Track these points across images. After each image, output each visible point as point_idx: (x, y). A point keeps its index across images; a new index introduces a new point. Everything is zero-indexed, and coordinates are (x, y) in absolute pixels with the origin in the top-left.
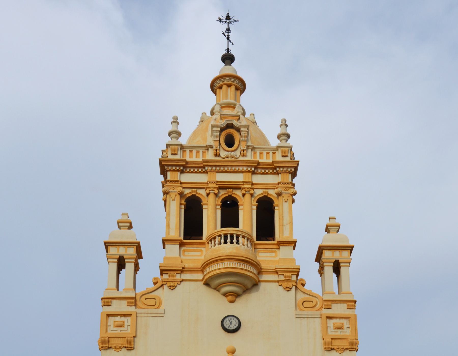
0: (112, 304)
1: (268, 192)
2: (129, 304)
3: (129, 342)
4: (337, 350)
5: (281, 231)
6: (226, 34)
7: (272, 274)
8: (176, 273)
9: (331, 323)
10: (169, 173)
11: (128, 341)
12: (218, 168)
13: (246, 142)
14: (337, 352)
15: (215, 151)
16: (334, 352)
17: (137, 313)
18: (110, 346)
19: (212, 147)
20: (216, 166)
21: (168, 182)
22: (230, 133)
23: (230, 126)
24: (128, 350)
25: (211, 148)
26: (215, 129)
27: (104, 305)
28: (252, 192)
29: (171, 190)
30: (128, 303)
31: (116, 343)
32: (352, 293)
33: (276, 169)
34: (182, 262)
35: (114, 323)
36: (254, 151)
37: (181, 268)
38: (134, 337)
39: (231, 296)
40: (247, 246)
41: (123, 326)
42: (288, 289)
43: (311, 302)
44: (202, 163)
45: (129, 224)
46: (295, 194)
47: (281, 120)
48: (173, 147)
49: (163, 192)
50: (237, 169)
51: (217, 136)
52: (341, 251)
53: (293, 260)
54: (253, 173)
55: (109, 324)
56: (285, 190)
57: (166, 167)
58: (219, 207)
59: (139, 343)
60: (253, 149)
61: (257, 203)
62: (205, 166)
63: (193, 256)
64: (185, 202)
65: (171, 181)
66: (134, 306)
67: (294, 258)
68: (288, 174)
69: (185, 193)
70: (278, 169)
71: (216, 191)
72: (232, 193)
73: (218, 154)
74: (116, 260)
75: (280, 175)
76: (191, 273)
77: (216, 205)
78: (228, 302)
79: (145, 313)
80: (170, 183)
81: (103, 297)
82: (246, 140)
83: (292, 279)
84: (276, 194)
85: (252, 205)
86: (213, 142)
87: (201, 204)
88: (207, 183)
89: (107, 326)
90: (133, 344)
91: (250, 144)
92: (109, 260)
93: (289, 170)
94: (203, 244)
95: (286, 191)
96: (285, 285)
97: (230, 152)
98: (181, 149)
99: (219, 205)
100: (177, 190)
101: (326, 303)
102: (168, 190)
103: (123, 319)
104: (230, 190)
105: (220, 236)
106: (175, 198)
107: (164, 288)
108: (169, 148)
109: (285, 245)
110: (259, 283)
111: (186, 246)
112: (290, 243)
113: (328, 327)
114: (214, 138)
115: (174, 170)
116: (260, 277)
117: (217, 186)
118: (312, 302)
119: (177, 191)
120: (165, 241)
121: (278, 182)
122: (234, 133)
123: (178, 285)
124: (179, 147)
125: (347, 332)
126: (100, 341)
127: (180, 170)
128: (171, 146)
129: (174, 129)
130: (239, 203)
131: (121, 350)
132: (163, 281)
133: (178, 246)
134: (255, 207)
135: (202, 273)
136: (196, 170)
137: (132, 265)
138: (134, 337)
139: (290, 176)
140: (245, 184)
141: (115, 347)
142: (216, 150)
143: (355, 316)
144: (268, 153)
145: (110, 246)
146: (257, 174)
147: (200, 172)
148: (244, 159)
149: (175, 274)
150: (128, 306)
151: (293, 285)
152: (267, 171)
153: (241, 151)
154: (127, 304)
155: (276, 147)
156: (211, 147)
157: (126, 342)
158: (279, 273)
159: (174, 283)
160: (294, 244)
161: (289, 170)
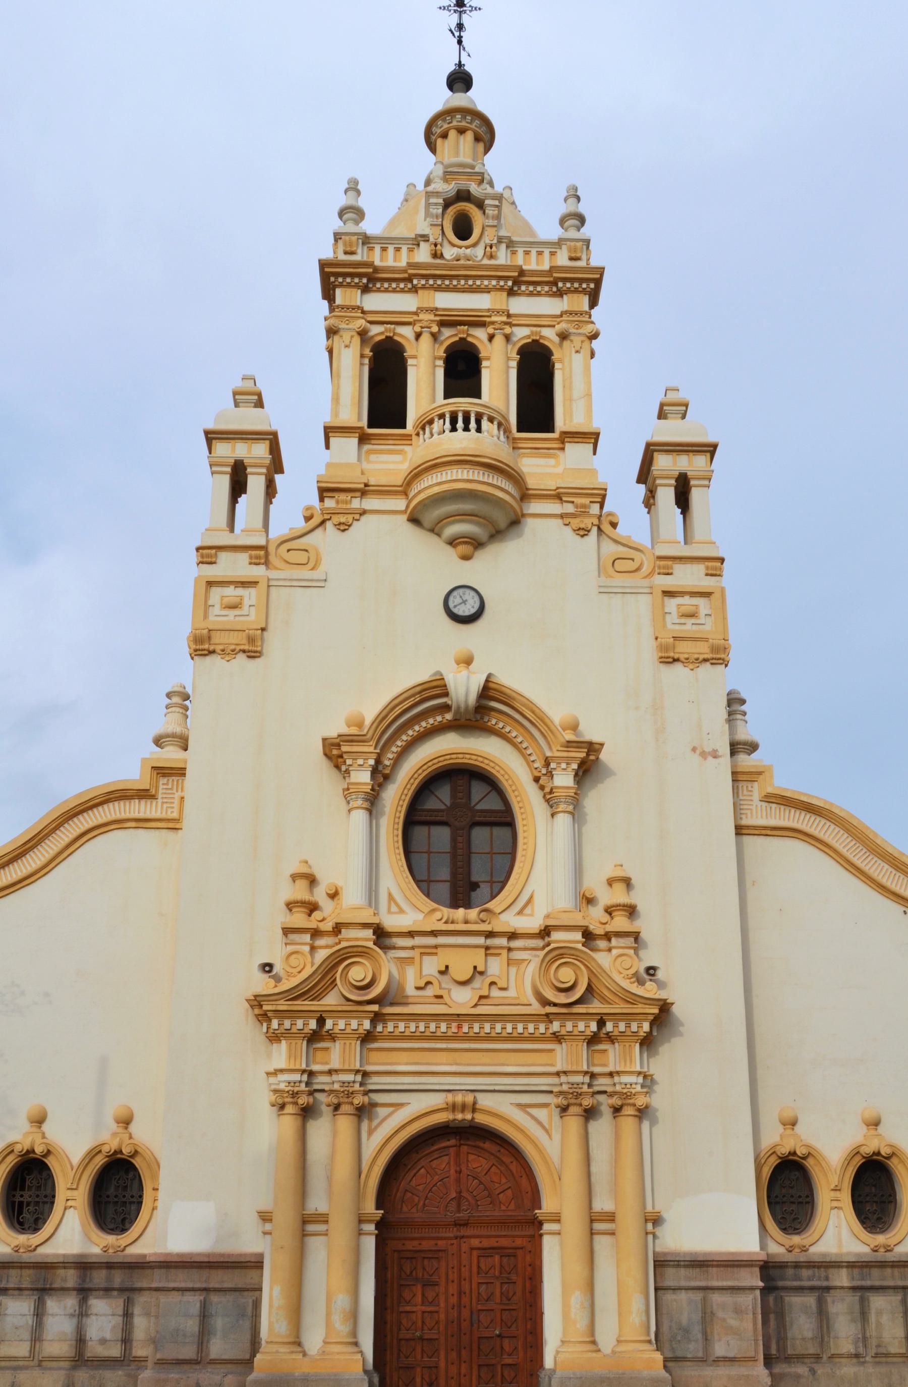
0: (218, 561)
1: (540, 332)
2: (253, 561)
4: (686, 662)
5: (568, 413)
6: (457, 34)
7: (548, 501)
8: (352, 497)
9: (672, 604)
10: (338, 291)
11: (249, 639)
12: (439, 282)
13: (495, 229)
14: (685, 666)
15: (433, 246)
16: (678, 667)
17: (269, 580)
18: (212, 648)
19: (428, 239)
20: (435, 277)
21: (336, 310)
22: (464, 210)
23: (463, 196)
24: (249, 657)
25: (424, 241)
26: (433, 200)
27: (202, 563)
28: (508, 330)
29: (343, 326)
30: (251, 557)
31: (226, 641)
32: (715, 543)
33: (556, 285)
34: (363, 473)
35: (222, 600)
36: (511, 249)
37: (362, 486)
38: (263, 630)
40: (498, 438)
41: (240, 606)
42: (582, 533)
43: (631, 561)
44: (405, 271)
45: (256, 397)
46: (594, 336)
47: (568, 187)
48: (347, 238)
49: (326, 329)
50: (478, 282)
51: (437, 217)
52: (691, 454)
53: (593, 472)
54: (511, 293)
55: (210, 602)
56: (576, 326)
57: (332, 279)
58: (441, 363)
59: (273, 643)
60: (511, 244)
61: (517, 354)
62: (413, 277)
63: (386, 462)
64: (371, 351)
65: (342, 307)
66: (263, 564)
67: (595, 467)
68: (581, 295)
69: (371, 334)
70: (560, 285)
71: (435, 329)
72: (468, 335)
73: (439, 252)
74: (229, 469)
75: (565, 296)
76: (382, 497)
77: (436, 358)
79: (285, 579)
80: (340, 311)
81: (199, 543)
82: (496, 224)
83: (591, 512)
84: (557, 335)
85: (508, 359)
86: (430, 227)
87: (404, 356)
88: (416, 313)
89: (207, 607)
90: (259, 643)
91: (503, 233)
92: (214, 469)
93: (584, 286)
94: (408, 437)
95: (577, 329)
96: (576, 523)
97: (463, 248)
98: (363, 244)
99: (440, 358)
100: (355, 325)
101: (662, 563)
102: (336, 325)
103: (240, 591)
104: (462, 327)
105: (442, 416)
106: (350, 342)
107: (325, 529)
108: (339, 240)
109: (576, 440)
110: (523, 520)
111: (373, 442)
112: (586, 436)
113: (666, 613)
114: (432, 220)
115: (349, 285)
116: (525, 506)
117: (438, 318)
118: (633, 560)
119: (355, 327)
120: (329, 430)
121: (562, 312)
122: (471, 211)
123: (355, 522)
124: (360, 239)
125: (707, 626)
126: (191, 639)
127: (361, 284)
128: (343, 237)
129: (351, 202)
130: (480, 353)
131: (235, 658)
132: (324, 512)
133: (355, 441)
134: (514, 364)
135: (404, 497)
136: (394, 285)
137: (262, 479)
138: (263, 630)
139: (585, 300)
140: (493, 314)
141: (223, 650)
142: (436, 245)
143: (723, 590)
144: (540, 253)
145: (217, 441)
146: (519, 295)
147: (402, 291)
148: (493, 262)
149: (349, 497)
150: (250, 563)
151: (592, 523)
152: (539, 289)
153: (486, 248)
155: (557, 241)
156: (425, 237)
157: (245, 641)
158: (564, 499)
159: (346, 516)
160: (595, 438)
161: (584, 286)
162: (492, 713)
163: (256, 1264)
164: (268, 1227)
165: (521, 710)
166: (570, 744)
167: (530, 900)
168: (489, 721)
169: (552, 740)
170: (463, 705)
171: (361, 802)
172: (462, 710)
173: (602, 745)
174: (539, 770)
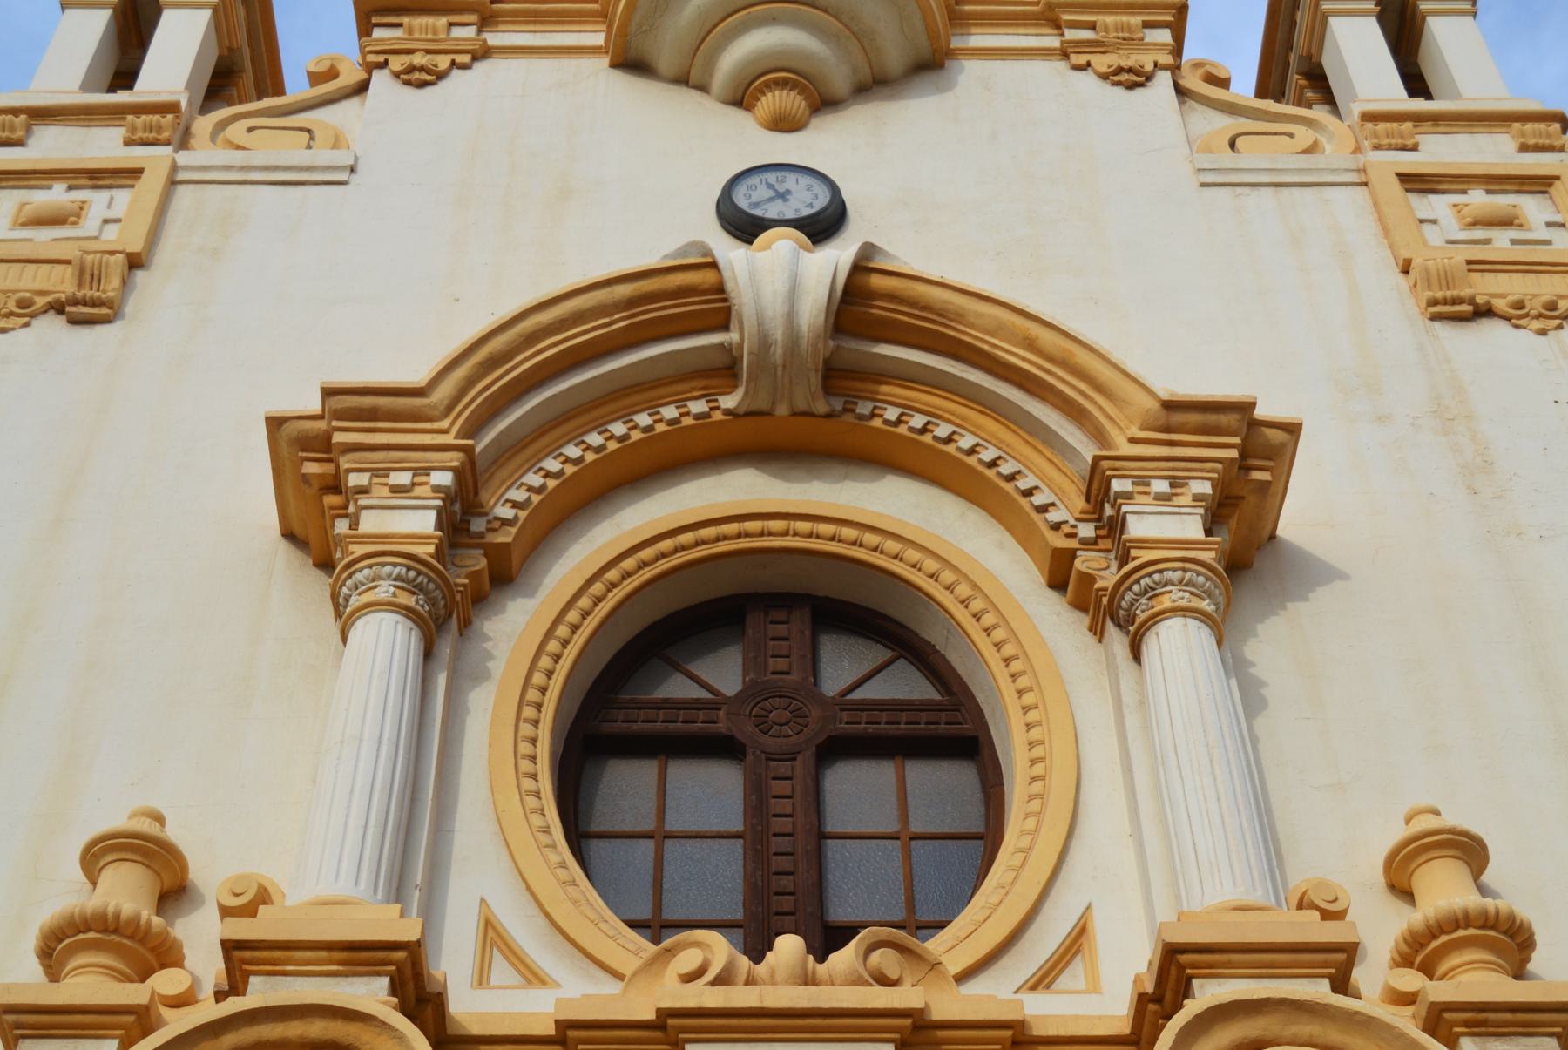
0: (30, 142)
3: (92, 276)
4: (1517, 314)
14: (1517, 326)
16: (1492, 332)
24: (75, 321)
39: (777, 93)
41: (72, 219)
78: (763, 130)
110: (948, 63)
113: (1422, 221)
131: (27, 325)
154: (129, 135)
162: (884, 388)
165: (986, 347)
166: (1178, 418)
167: (1077, 942)
168: (873, 415)
169: (1110, 418)
170: (778, 334)
171: (392, 589)
172: (778, 353)
173: (1293, 429)
174: (1066, 529)
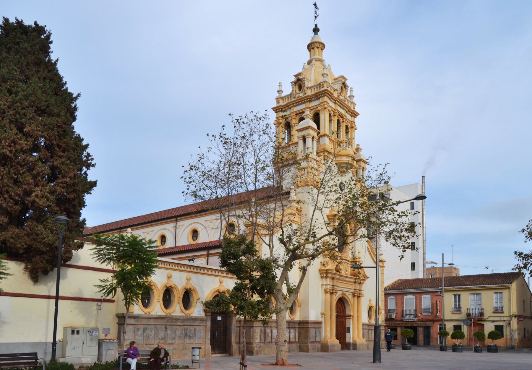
147: (333, 102)
156: (337, 90)
163: (320, 323)
164: (324, 316)
